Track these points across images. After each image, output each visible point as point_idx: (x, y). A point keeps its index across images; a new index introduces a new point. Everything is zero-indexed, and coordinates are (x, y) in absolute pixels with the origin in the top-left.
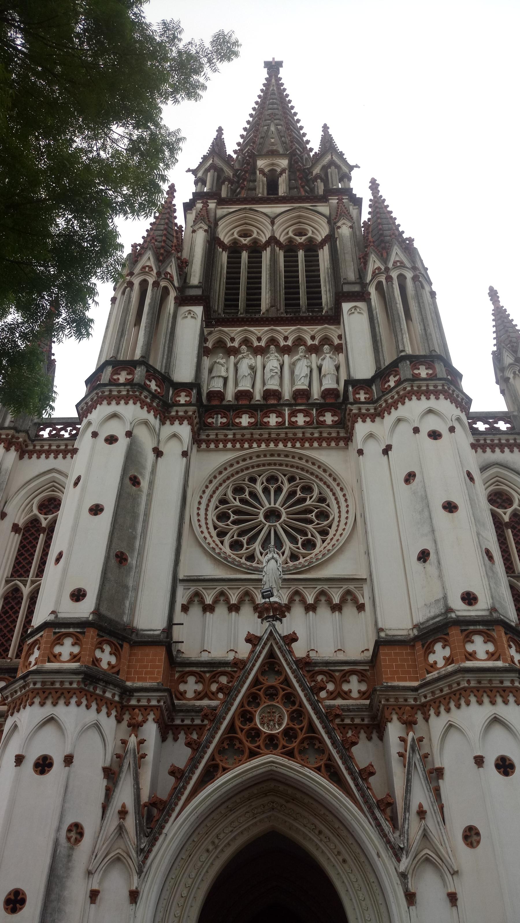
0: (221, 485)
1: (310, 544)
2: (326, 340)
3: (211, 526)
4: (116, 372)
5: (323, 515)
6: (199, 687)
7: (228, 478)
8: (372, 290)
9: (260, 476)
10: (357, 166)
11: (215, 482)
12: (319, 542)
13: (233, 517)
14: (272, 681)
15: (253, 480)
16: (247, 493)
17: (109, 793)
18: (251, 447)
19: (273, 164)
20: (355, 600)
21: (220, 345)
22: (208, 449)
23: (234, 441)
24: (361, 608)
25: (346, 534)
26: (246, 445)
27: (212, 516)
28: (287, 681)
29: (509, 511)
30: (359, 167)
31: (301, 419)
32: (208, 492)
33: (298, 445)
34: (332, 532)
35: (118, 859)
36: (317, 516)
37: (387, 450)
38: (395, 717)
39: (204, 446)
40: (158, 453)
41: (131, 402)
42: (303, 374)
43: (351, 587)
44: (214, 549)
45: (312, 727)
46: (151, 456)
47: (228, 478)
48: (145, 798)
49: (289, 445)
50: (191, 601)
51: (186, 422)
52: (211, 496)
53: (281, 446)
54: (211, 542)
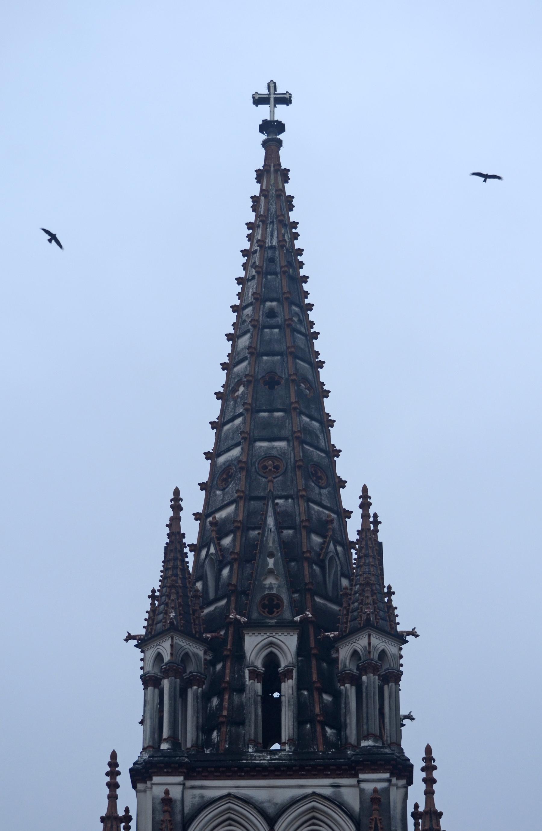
10: (413, 633)
19: (271, 644)
30: (417, 636)
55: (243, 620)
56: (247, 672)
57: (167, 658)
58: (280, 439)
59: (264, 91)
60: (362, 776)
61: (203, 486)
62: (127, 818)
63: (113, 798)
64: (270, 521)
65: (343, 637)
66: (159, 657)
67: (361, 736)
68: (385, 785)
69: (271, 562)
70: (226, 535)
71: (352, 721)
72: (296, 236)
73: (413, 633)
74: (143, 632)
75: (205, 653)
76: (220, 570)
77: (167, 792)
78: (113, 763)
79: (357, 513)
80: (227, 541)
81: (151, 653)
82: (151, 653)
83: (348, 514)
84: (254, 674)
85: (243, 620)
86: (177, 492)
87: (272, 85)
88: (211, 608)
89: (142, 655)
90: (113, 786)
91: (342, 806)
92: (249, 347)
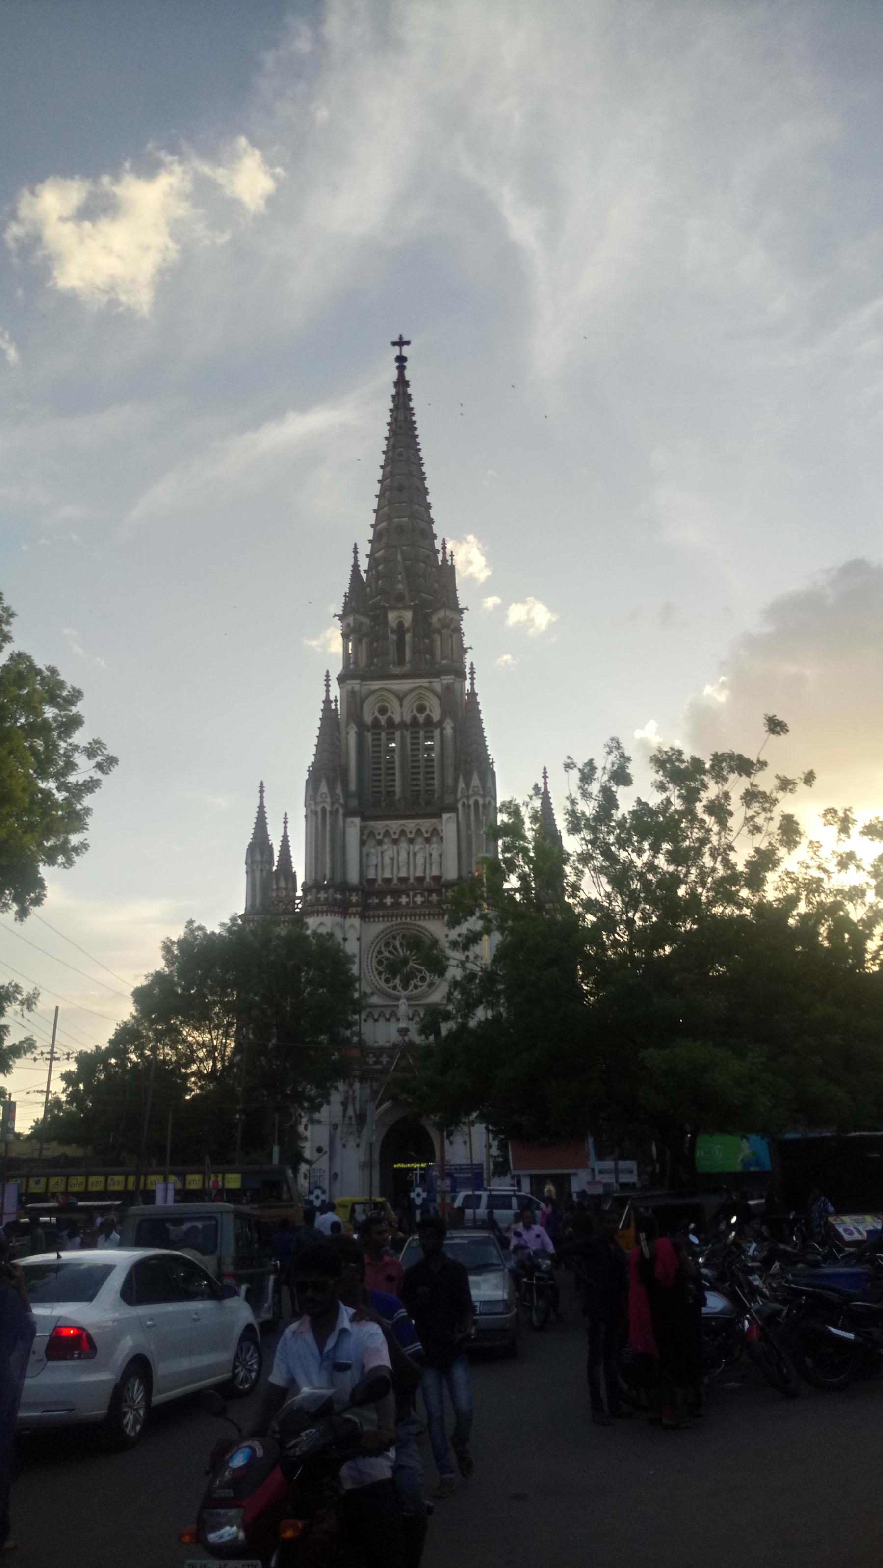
0: (377, 943)
2: (435, 832)
3: (374, 970)
4: (318, 892)
6: (374, 1059)
7: (381, 939)
8: (460, 806)
10: (467, 609)
15: (394, 937)
17: (345, 1110)
18: (392, 920)
19: (400, 617)
21: (372, 834)
22: (369, 921)
23: (383, 916)
26: (390, 919)
27: (374, 964)
31: (419, 899)
32: (372, 950)
33: (417, 918)
35: (351, 1133)
39: (367, 920)
41: (329, 914)
44: (376, 987)
47: (381, 939)
48: (358, 1113)
51: (357, 916)
52: (373, 951)
53: (408, 920)
55: (387, 605)
56: (389, 631)
57: (352, 624)
58: (404, 517)
59: (397, 340)
60: (442, 677)
61: (370, 541)
62: (336, 701)
63: (328, 691)
64: (399, 558)
65: (435, 610)
66: (349, 624)
67: (443, 658)
68: (452, 681)
69: (400, 577)
70: (379, 565)
71: (438, 651)
72: (413, 414)
73: (467, 609)
74: (341, 613)
75: (371, 622)
76: (377, 582)
77: (353, 688)
78: (327, 676)
79: (441, 551)
80: (380, 567)
81: (345, 622)
82: (345, 622)
83: (438, 551)
84: (393, 631)
85: (387, 605)
86: (355, 545)
87: (401, 337)
88: (374, 600)
90: (328, 686)
91: (433, 691)
92: (390, 472)
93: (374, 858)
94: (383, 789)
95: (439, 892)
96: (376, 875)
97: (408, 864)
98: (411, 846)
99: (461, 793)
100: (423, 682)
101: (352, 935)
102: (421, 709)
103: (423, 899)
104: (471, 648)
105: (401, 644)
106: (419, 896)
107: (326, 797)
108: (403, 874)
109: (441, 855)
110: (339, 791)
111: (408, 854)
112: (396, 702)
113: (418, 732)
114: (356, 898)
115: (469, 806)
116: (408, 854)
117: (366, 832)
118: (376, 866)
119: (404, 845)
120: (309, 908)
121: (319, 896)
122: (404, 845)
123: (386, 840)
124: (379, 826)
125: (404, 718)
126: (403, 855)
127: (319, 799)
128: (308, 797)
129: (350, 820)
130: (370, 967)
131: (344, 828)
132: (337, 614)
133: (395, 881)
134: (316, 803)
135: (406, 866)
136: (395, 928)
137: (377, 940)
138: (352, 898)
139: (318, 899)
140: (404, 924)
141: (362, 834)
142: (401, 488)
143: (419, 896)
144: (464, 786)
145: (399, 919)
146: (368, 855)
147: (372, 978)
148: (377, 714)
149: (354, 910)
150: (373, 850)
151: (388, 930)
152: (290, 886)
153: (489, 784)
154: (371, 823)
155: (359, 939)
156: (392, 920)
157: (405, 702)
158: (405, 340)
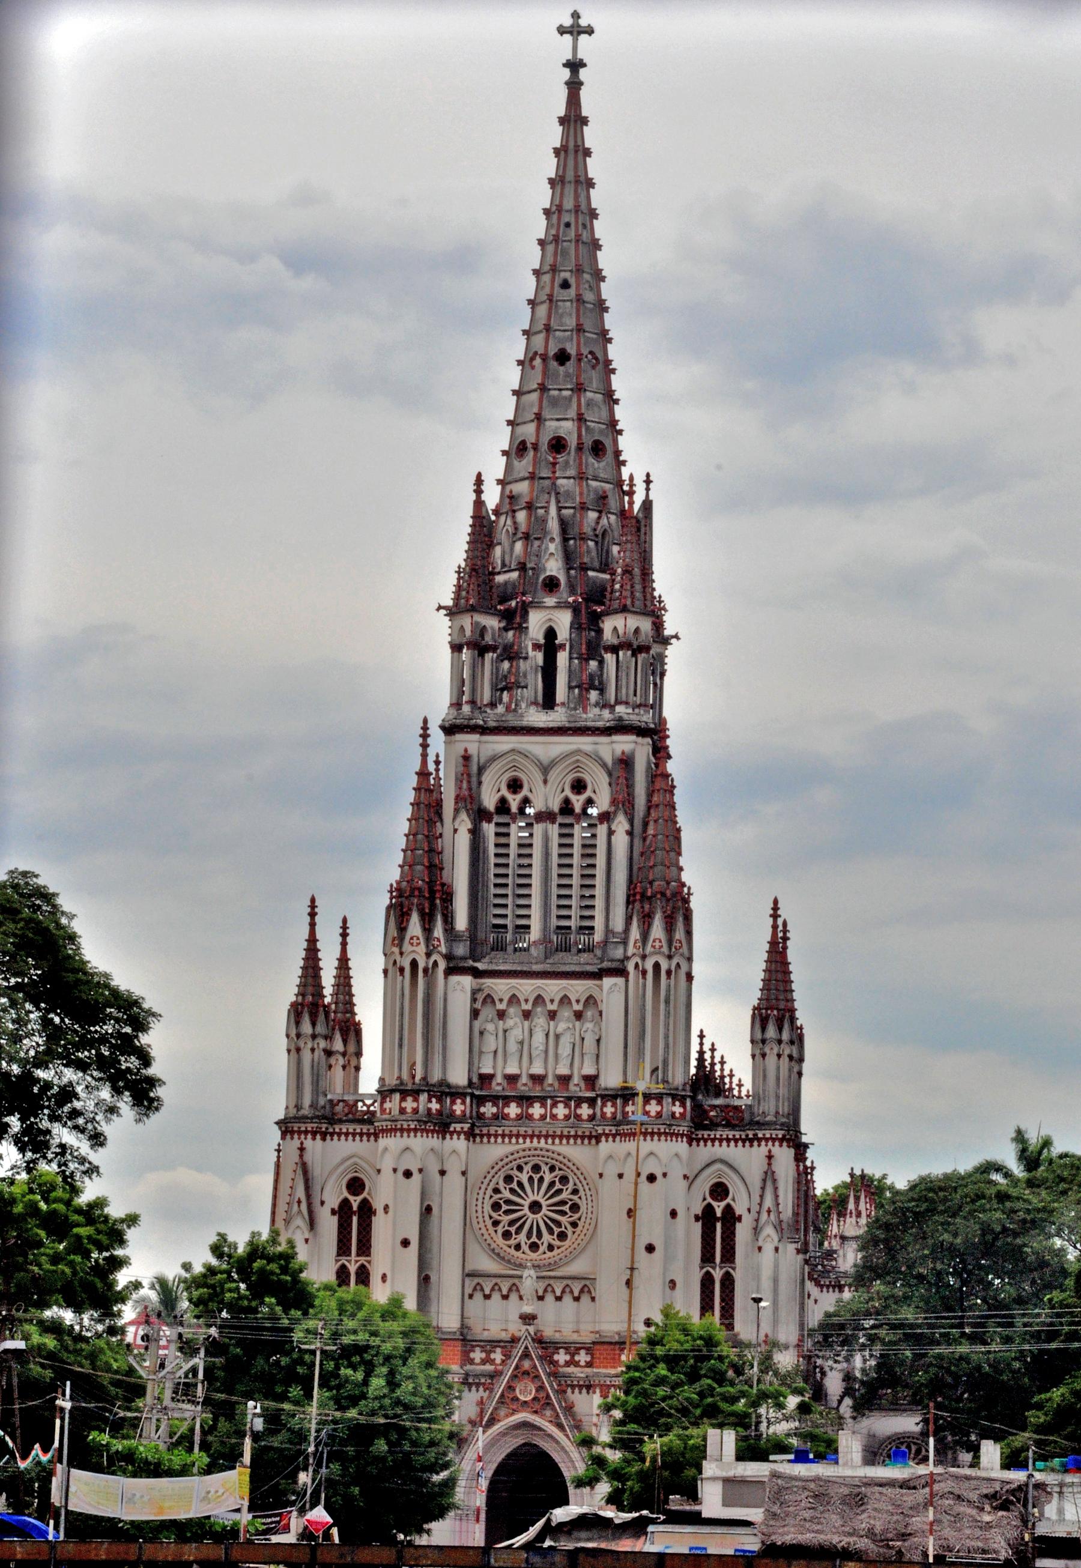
1: (562, 1236)
2: (591, 1001)
3: (487, 1218)
4: (403, 1099)
5: (575, 1208)
9: (526, 1164)
11: (489, 1177)
12: (569, 1234)
13: (505, 1207)
14: (526, 1365)
15: (520, 1168)
16: (515, 1183)
19: (550, 620)
20: (589, 1292)
21: (489, 999)
24: (593, 1299)
25: (589, 1233)
26: (514, 1140)
28: (535, 1367)
29: (723, 1204)
31: (561, 1111)
32: (483, 1187)
34: (581, 1224)
36: (571, 1208)
37: (621, 1176)
38: (598, 1391)
39: (478, 1139)
40: (442, 1173)
41: (419, 1134)
42: (565, 1054)
43: (588, 1283)
45: (548, 1397)
46: (438, 1176)
49: (550, 1141)
50: (475, 1289)
54: (488, 1238)
59: (568, 22)
74: (450, 603)
77: (466, 750)
84: (536, 647)
86: (479, 475)
89: (449, 624)
93: (492, 1038)
94: (508, 922)
95: (592, 1102)
96: (494, 1067)
97: (546, 1052)
98: (552, 1023)
99: (635, 946)
100: (584, 743)
101: (454, 1168)
102: (579, 786)
103: (566, 1111)
104: (676, 637)
105: (549, 671)
106: (561, 1106)
107: (419, 944)
108: (537, 1069)
109: (598, 1041)
110: (438, 932)
111: (547, 1035)
112: (538, 777)
113: (571, 825)
114: (463, 1107)
115: (644, 973)
116: (547, 1035)
117: (480, 997)
118: (495, 1052)
119: (540, 1020)
120: (389, 1123)
121: (404, 1105)
122: (540, 1020)
123: (512, 1011)
124: (501, 987)
125: (550, 805)
126: (539, 1038)
127: (407, 947)
128: (389, 940)
129: (455, 979)
130: (480, 1214)
131: (445, 994)
132: (442, 604)
133: (524, 1079)
134: (401, 954)
135: (543, 1055)
136: (522, 1154)
137: (493, 1172)
138: (455, 1107)
139: (402, 1111)
140: (536, 1149)
141: (474, 1000)
142: (562, 357)
143: (561, 1106)
144: (638, 937)
145: (528, 1140)
146: (481, 1033)
147: (484, 1231)
148: (505, 792)
149: (458, 1127)
150: (490, 1027)
151: (511, 1158)
152: (352, 1048)
153: (679, 934)
154: (488, 982)
155: (464, 1173)
156: (517, 1142)
157: (553, 776)
158: (583, 22)
